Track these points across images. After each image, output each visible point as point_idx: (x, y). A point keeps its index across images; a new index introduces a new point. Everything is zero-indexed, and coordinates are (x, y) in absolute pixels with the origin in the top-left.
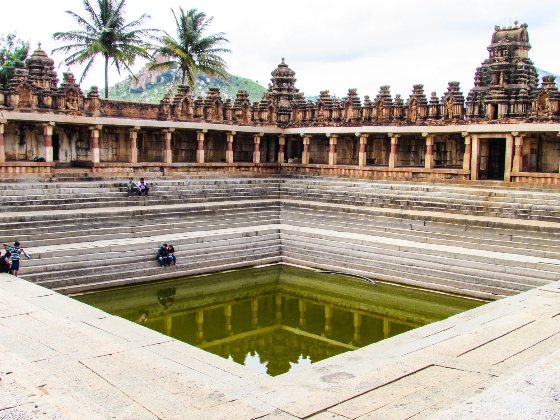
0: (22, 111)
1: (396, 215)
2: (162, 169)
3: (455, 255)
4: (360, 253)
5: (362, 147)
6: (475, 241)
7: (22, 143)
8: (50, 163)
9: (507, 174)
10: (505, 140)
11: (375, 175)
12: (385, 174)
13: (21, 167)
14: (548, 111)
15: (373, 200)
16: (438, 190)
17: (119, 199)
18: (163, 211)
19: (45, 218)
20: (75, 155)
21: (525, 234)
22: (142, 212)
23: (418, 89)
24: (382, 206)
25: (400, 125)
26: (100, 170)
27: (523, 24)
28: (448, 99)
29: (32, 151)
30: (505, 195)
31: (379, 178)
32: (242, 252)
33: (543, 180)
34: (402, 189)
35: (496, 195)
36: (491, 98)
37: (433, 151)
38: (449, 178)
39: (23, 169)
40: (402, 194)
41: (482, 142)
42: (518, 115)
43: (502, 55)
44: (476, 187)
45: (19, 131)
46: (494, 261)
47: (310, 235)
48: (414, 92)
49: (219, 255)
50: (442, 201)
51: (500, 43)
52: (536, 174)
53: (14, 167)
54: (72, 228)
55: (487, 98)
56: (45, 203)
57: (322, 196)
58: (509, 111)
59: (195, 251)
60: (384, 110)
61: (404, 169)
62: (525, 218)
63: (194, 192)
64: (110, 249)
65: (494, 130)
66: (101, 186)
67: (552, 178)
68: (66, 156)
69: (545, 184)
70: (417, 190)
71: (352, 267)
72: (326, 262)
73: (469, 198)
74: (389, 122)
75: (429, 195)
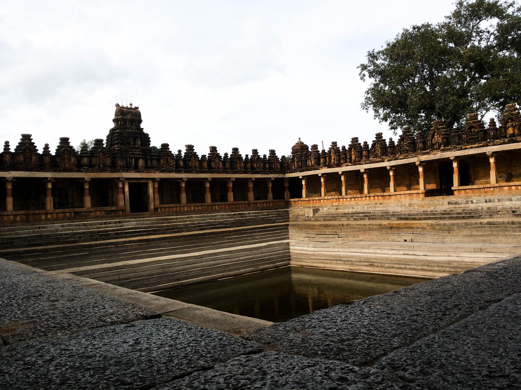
1: (139, 241)
3: (231, 252)
4: (176, 268)
5: (9, 192)
6: (213, 245)
9: (152, 207)
10: (146, 185)
11: (30, 219)
12: (43, 217)
14: (172, 166)
15: (80, 237)
16: (129, 221)
21: (229, 235)
23: (65, 141)
24: (96, 240)
25: (55, 171)
27: (137, 106)
28: (99, 152)
30: (177, 219)
31: (39, 221)
33: (175, 209)
34: (96, 225)
35: (171, 219)
36: (134, 154)
37: (53, 195)
38: (110, 214)
40: (101, 228)
41: (130, 185)
42: (154, 167)
43: (132, 125)
44: (135, 218)
46: (251, 249)
47: (109, 269)
48: (60, 143)
50: (141, 228)
51: (129, 116)
52: (171, 205)
55: (131, 154)
57: (12, 243)
58: (146, 164)
60: (34, 158)
61: (66, 210)
62: (204, 229)
65: (144, 177)
67: (180, 207)
69: (176, 211)
70: (110, 223)
71: (184, 280)
72: (160, 283)
73: (158, 223)
74: (41, 168)
75: (127, 225)
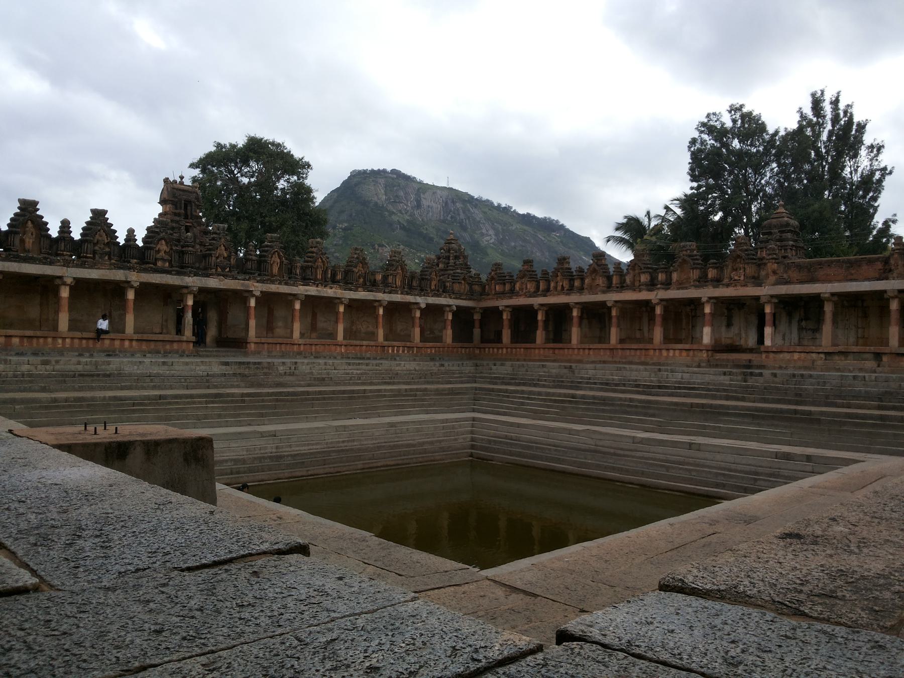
0: (678, 289)
2: (878, 356)
7: (729, 325)
8: (706, 346)
13: (674, 350)
17: (736, 392)
18: (735, 408)
19: (594, 397)
20: (797, 339)
22: (703, 405)
26: (771, 355)
29: (740, 334)
32: (731, 477)
39: (677, 352)
45: (726, 311)
49: (690, 470)
53: (668, 350)
54: (603, 411)
56: (638, 386)
59: (662, 457)
63: (866, 392)
64: (578, 432)
66: (725, 374)
68: (784, 339)
